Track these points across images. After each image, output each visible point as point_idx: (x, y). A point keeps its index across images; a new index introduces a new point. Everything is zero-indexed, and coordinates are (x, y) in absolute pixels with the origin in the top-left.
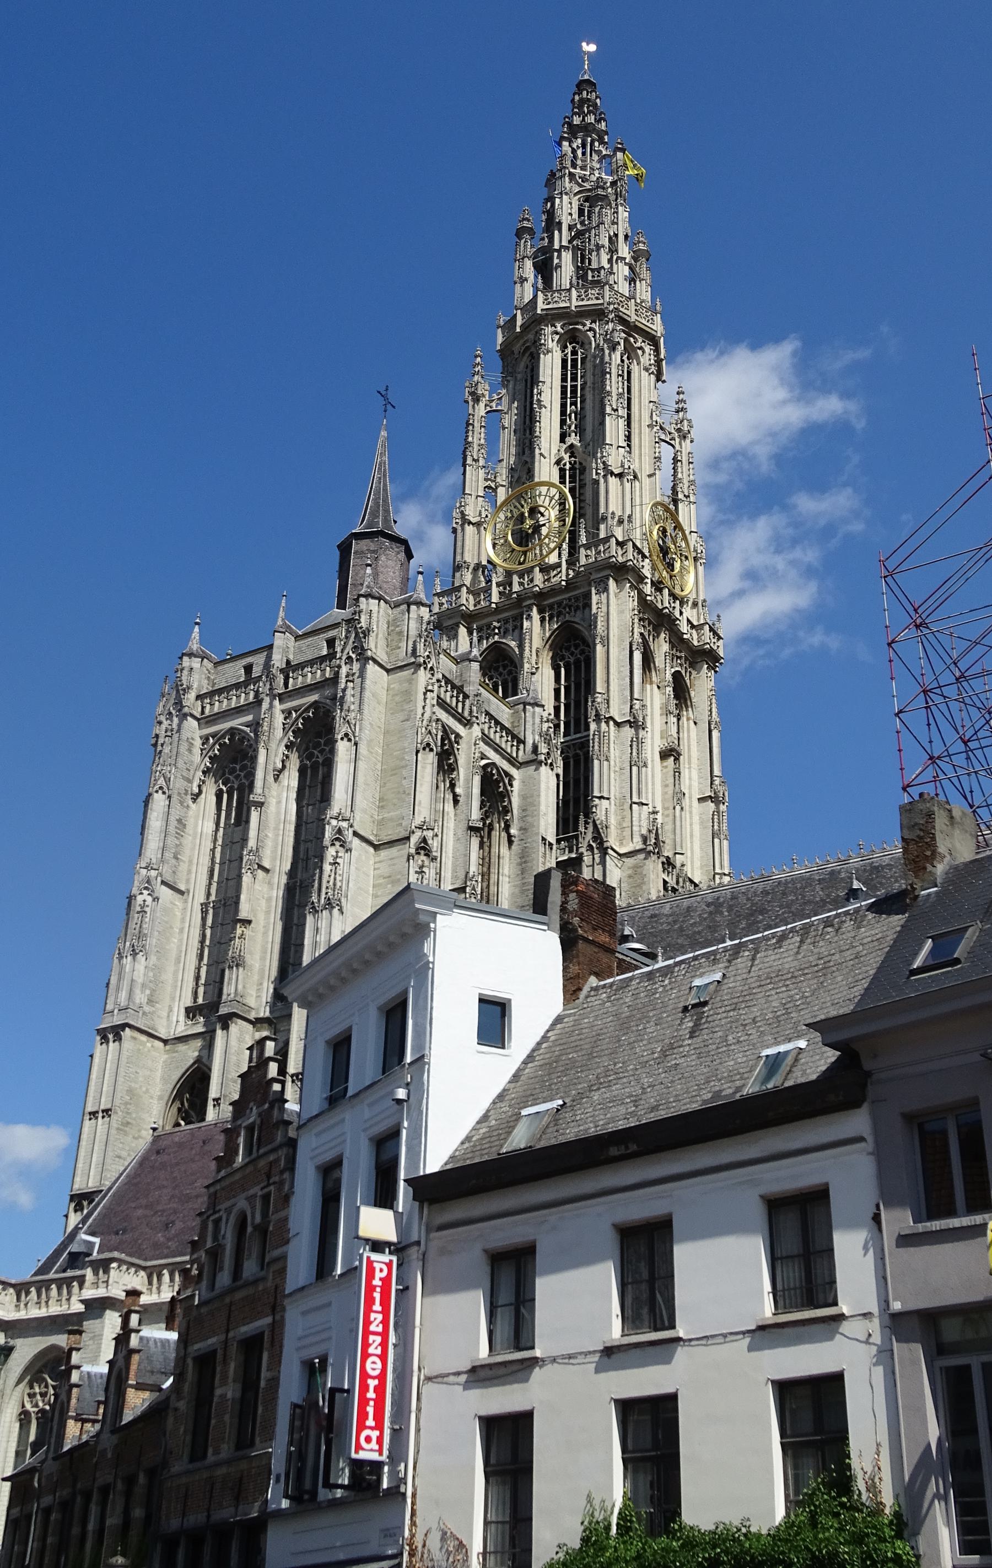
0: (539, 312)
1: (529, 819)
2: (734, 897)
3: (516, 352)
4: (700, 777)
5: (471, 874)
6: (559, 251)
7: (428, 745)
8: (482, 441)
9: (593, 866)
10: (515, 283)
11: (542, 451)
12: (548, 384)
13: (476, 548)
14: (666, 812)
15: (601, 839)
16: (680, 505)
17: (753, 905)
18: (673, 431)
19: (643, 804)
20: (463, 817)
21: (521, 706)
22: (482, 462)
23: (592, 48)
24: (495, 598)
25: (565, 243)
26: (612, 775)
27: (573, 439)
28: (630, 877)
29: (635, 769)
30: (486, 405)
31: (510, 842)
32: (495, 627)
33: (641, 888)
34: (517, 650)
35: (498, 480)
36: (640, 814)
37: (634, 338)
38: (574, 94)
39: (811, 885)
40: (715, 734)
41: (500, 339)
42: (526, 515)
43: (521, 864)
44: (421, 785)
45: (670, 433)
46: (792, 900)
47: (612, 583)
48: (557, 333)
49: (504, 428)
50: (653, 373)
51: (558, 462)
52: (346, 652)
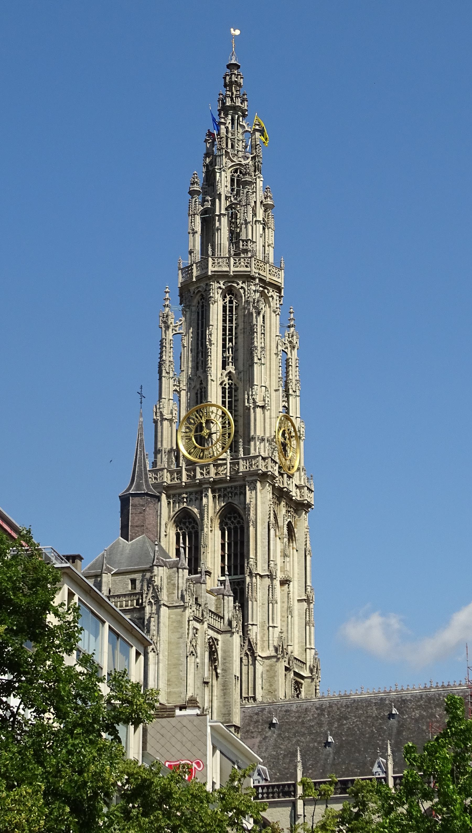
0: (210, 273)
1: (227, 664)
2: (330, 706)
3: (192, 292)
4: (299, 586)
5: (205, 708)
6: (219, 216)
7: (192, 652)
8: (171, 359)
9: (248, 665)
10: (189, 233)
11: (212, 378)
12: (215, 327)
13: (170, 437)
14: (283, 619)
15: (253, 651)
16: (291, 398)
17: (341, 713)
18: (286, 342)
19: (275, 627)
20: (200, 675)
21: (221, 596)
22: (171, 375)
23: (237, 32)
24: (184, 479)
25: (223, 212)
26: (258, 609)
27: (231, 368)
28: (268, 671)
29: (271, 605)
30: (173, 330)
31: (217, 677)
32: (184, 498)
33: (274, 679)
34: (198, 515)
35: (181, 386)
36: (273, 633)
37: (268, 289)
38: (226, 75)
39: (371, 706)
40: (308, 558)
41: (180, 279)
42: (204, 425)
43: (223, 690)
44: (190, 675)
45: (285, 344)
46: (361, 714)
47: (258, 484)
48: (220, 288)
49: (184, 347)
50: (278, 314)
51: (221, 384)
52: (148, 598)
